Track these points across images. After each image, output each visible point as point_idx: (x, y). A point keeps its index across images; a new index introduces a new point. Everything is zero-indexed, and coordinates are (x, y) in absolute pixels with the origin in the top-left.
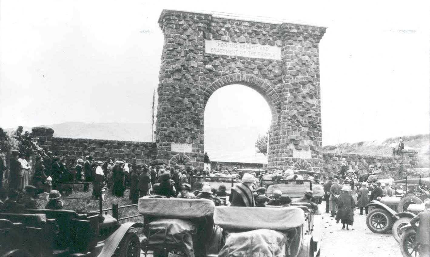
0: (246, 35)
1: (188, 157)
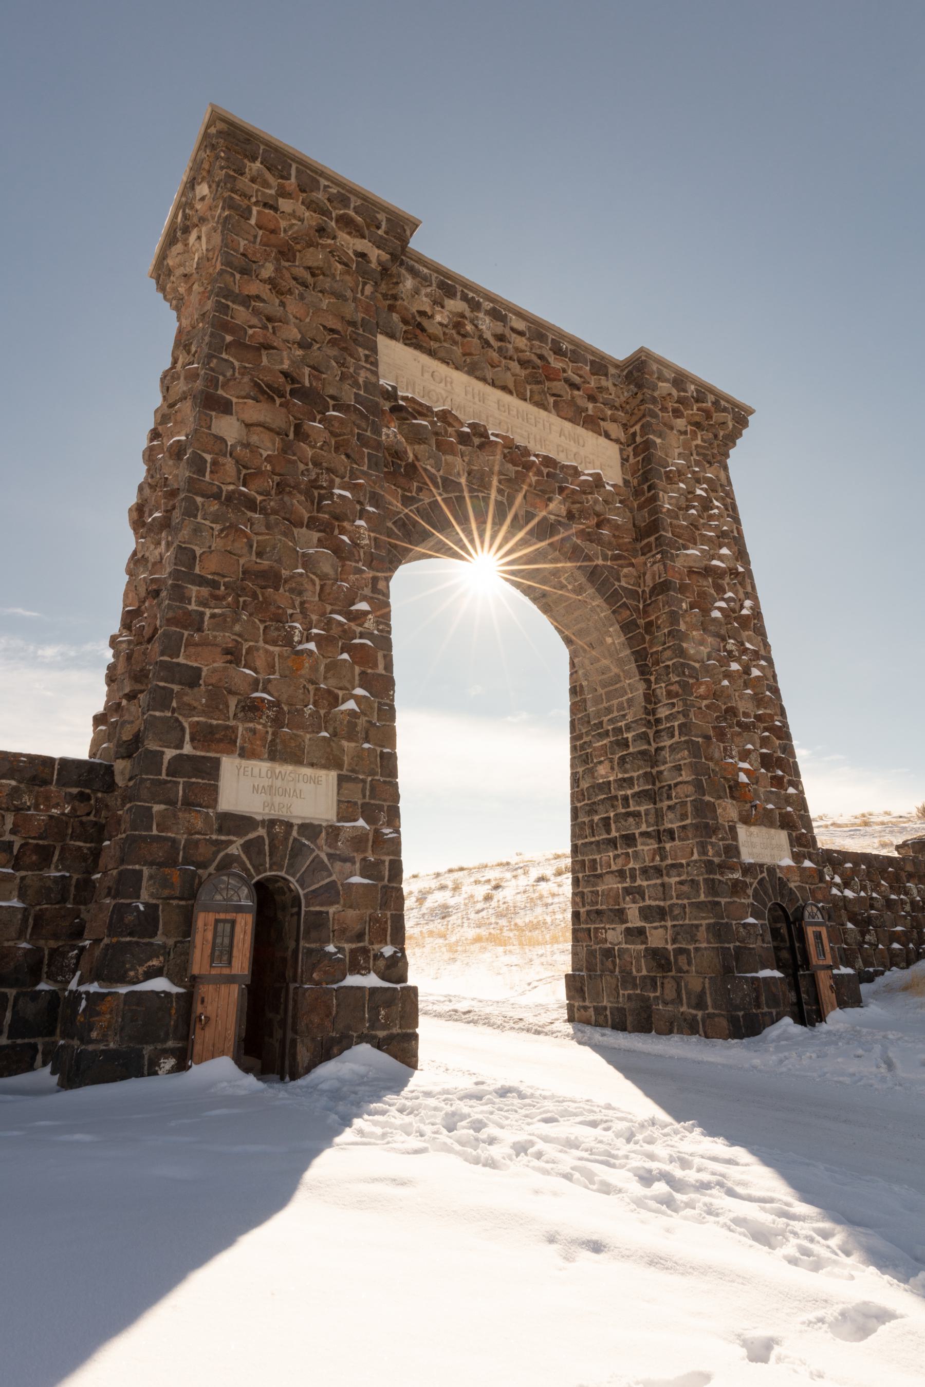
1: (317, 852)
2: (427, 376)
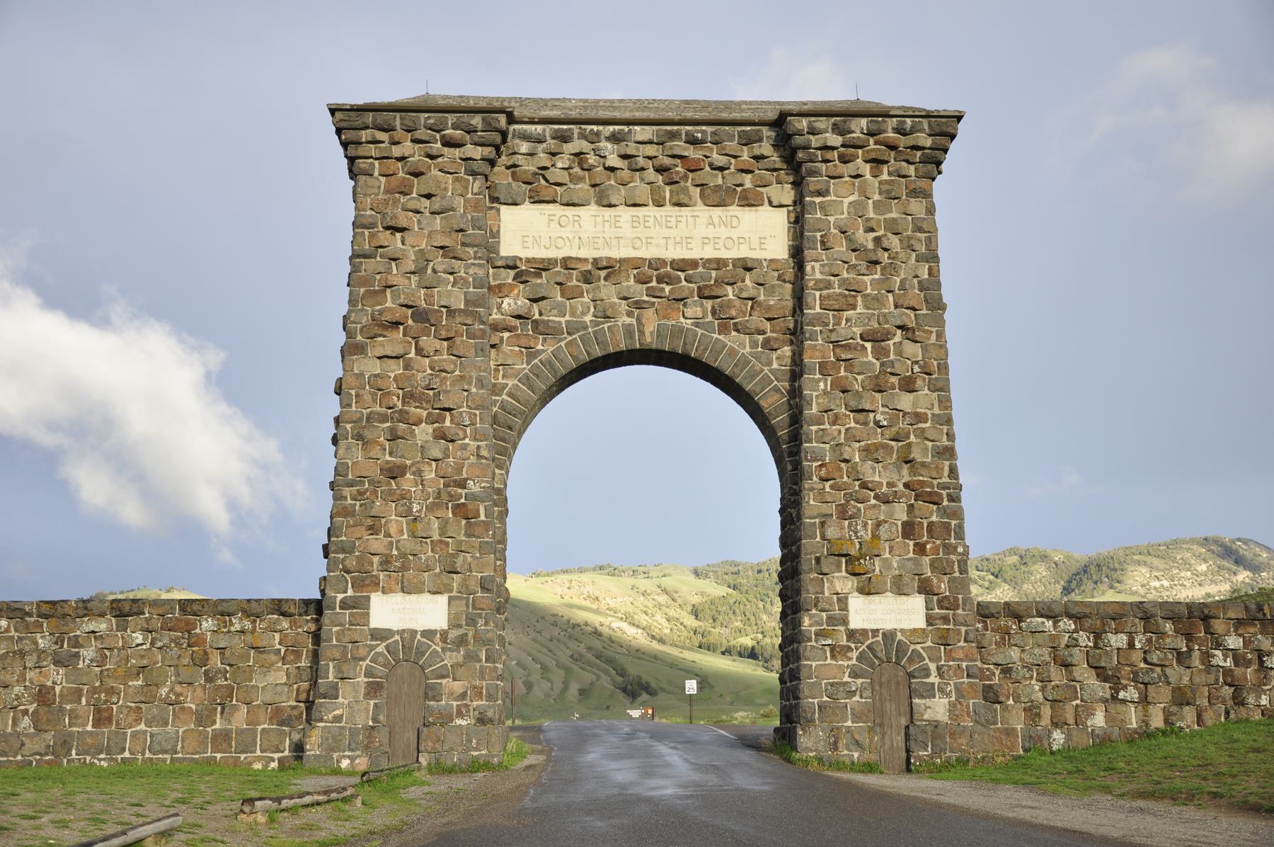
0: (651, 174)
1: (434, 646)
2: (554, 225)
